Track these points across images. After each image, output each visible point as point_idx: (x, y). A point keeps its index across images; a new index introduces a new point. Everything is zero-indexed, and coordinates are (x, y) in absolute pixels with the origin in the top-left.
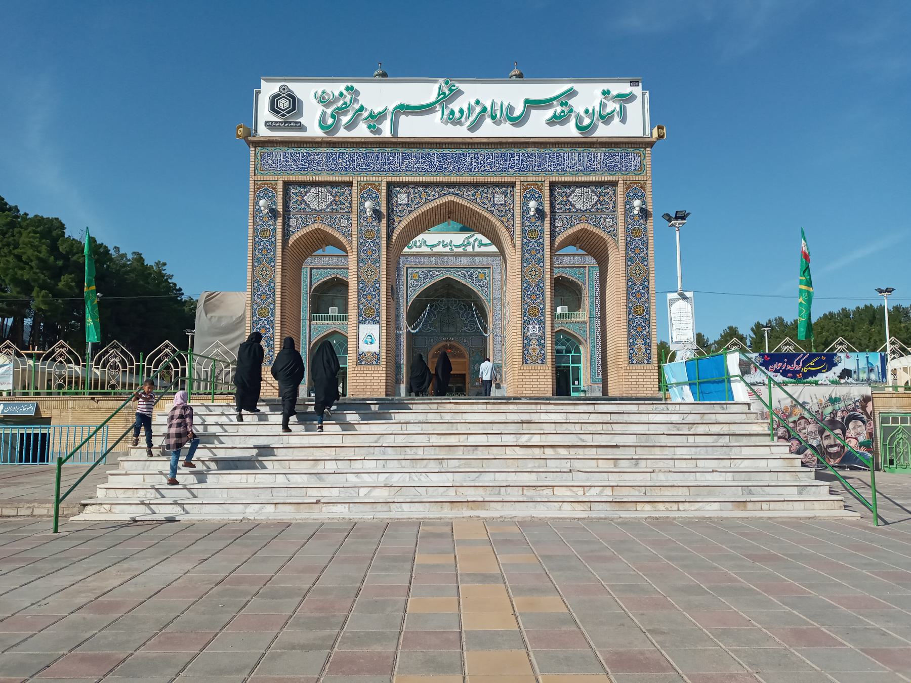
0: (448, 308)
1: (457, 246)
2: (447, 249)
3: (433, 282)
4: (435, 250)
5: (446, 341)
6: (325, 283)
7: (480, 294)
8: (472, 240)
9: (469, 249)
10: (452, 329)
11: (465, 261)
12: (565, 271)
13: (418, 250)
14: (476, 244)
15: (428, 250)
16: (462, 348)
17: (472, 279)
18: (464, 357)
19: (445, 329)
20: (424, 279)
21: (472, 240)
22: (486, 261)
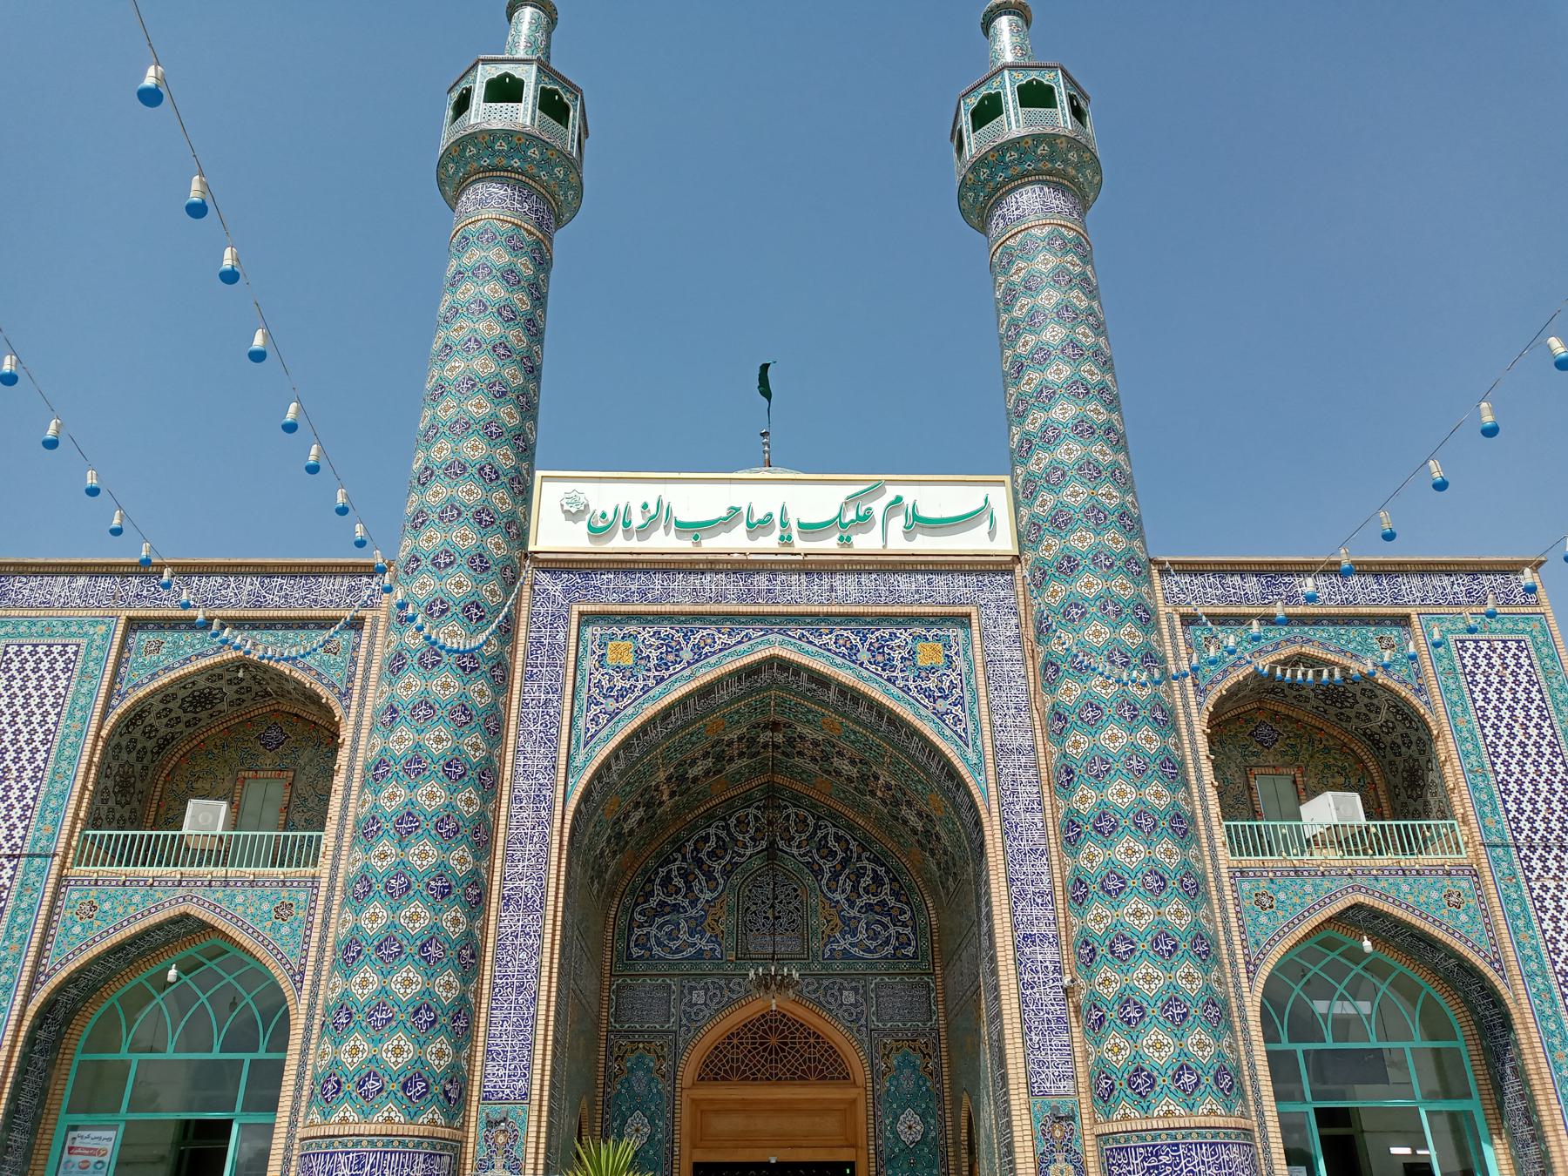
0: (772, 843)
1: (808, 529)
2: (769, 543)
3: (705, 676)
4: (715, 544)
5: (764, 983)
6: (196, 699)
7: (928, 730)
8: (878, 507)
9: (866, 542)
10: (787, 943)
11: (849, 593)
12: (1319, 633)
13: (635, 544)
14: (897, 523)
15: (686, 545)
16: (837, 1034)
17: (888, 665)
18: (845, 1077)
19: (760, 943)
20: (663, 664)
21: (878, 507)
22: (943, 593)
